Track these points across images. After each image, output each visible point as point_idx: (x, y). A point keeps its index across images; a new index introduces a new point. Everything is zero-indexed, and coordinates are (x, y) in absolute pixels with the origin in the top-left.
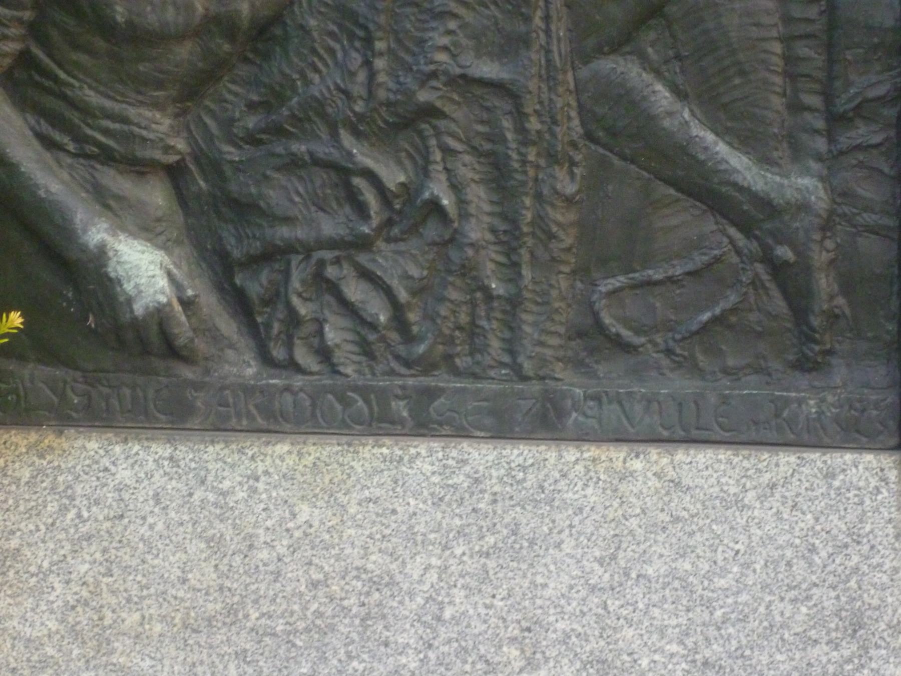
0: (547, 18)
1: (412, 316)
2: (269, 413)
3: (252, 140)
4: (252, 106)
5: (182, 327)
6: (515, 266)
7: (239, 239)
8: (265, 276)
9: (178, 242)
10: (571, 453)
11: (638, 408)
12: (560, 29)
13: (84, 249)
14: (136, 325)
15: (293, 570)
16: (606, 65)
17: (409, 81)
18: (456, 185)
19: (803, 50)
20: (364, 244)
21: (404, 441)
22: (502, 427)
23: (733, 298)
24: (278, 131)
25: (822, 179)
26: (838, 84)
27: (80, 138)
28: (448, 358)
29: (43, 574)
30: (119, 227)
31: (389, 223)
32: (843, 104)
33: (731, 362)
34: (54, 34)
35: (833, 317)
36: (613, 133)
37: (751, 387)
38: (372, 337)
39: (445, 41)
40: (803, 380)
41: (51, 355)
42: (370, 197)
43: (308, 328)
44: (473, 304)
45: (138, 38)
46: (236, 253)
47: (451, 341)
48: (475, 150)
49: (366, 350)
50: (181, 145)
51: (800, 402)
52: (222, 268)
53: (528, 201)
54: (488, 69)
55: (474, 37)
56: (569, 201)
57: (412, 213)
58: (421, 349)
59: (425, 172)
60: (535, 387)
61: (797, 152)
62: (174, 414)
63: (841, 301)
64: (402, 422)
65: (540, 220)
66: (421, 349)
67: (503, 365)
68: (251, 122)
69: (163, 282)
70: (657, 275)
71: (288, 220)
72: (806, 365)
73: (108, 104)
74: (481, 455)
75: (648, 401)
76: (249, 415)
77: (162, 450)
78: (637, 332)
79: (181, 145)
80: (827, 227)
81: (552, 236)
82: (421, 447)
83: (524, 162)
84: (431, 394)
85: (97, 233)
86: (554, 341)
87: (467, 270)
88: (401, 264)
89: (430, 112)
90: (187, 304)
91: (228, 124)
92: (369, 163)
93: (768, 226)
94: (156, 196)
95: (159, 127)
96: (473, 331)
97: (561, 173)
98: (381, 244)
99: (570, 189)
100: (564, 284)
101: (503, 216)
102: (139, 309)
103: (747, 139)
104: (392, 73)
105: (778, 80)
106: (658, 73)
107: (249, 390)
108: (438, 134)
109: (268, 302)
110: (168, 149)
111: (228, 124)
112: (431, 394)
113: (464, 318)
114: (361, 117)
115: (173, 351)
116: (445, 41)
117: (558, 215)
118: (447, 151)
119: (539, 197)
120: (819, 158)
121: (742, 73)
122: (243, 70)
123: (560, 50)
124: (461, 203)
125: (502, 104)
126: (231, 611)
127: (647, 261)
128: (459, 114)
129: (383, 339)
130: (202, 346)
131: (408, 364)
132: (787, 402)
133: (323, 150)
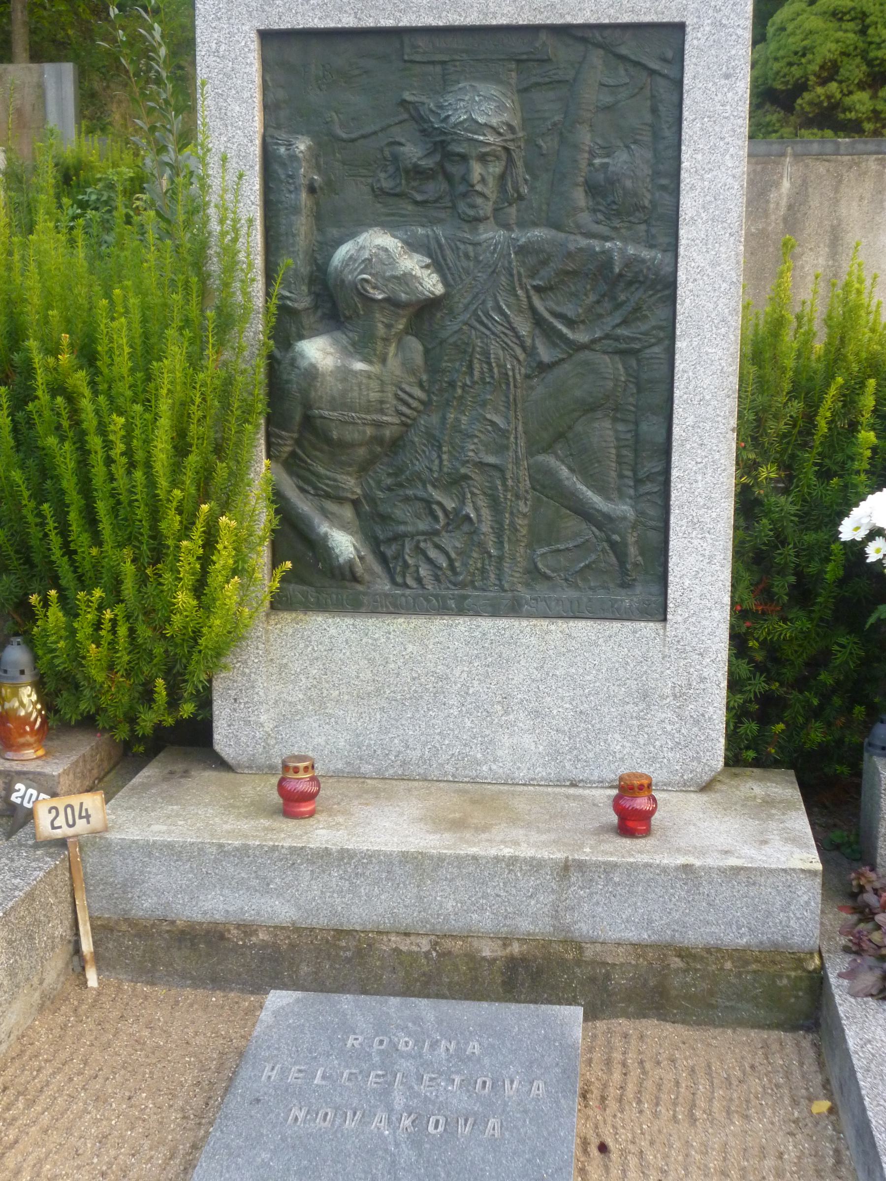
0: (516, 438)
1: (457, 564)
2: (395, 606)
3: (389, 489)
4: (389, 475)
5: (359, 569)
6: (501, 543)
7: (383, 531)
8: (394, 547)
9: (357, 533)
10: (525, 623)
11: (553, 603)
12: (522, 443)
13: (318, 534)
14: (340, 567)
15: (405, 673)
16: (541, 458)
17: (457, 464)
18: (477, 509)
19: (625, 452)
20: (436, 533)
21: (453, 618)
22: (495, 612)
24: (401, 485)
25: (632, 506)
26: (639, 466)
27: (316, 488)
28: (472, 582)
29: (297, 674)
30: (332, 525)
31: (448, 524)
32: (641, 475)
33: (592, 584)
34: (306, 443)
35: (636, 565)
36: (544, 487)
37: (601, 595)
38: (440, 573)
39: (472, 447)
40: (623, 592)
41: (302, 581)
42: (440, 514)
43: (412, 569)
44: (483, 559)
45: (343, 445)
46: (381, 537)
47: (473, 575)
48: (485, 494)
49: (437, 579)
50: (359, 491)
51: (622, 601)
52: (374, 543)
53: (507, 515)
54: (491, 459)
55: (485, 445)
56: (525, 515)
58: (461, 578)
59: (463, 503)
60: (510, 594)
61: (622, 496)
62: (354, 606)
63: (640, 558)
64: (452, 610)
65: (512, 524)
66: (461, 578)
67: (495, 585)
68: (389, 481)
69: (352, 549)
70: (561, 547)
71: (405, 523)
72: (624, 585)
73: (328, 473)
74: (486, 624)
75: (558, 600)
76: (387, 606)
77: (349, 621)
78: (553, 571)
79: (359, 491)
80: (634, 527)
81: (517, 530)
82: (460, 620)
83: (506, 499)
84: (465, 597)
85: (324, 528)
86: (517, 575)
87: (481, 545)
88: (452, 542)
89: (466, 477)
90: (361, 558)
91: (379, 482)
92: (439, 499)
93: (609, 526)
94: (348, 513)
95: (350, 484)
96: (483, 571)
97: (521, 503)
98: (444, 533)
99: (525, 510)
100: (522, 550)
101: (496, 522)
102: (341, 560)
103: (602, 489)
104: (450, 461)
105: (614, 465)
106: (563, 462)
107: (386, 596)
108: (469, 487)
110: (353, 493)
111: (379, 482)
112: (465, 597)
113: (479, 565)
114: (436, 479)
115: (355, 579)
116: (472, 447)
117: (520, 521)
118: (473, 494)
119: (512, 513)
120: (631, 498)
121: (599, 462)
122: (386, 460)
124: (479, 515)
125: (496, 474)
126: (378, 690)
127: (558, 541)
128: (477, 477)
129: (444, 574)
130: (367, 577)
131: (455, 585)
132: (616, 601)
133: (420, 493)
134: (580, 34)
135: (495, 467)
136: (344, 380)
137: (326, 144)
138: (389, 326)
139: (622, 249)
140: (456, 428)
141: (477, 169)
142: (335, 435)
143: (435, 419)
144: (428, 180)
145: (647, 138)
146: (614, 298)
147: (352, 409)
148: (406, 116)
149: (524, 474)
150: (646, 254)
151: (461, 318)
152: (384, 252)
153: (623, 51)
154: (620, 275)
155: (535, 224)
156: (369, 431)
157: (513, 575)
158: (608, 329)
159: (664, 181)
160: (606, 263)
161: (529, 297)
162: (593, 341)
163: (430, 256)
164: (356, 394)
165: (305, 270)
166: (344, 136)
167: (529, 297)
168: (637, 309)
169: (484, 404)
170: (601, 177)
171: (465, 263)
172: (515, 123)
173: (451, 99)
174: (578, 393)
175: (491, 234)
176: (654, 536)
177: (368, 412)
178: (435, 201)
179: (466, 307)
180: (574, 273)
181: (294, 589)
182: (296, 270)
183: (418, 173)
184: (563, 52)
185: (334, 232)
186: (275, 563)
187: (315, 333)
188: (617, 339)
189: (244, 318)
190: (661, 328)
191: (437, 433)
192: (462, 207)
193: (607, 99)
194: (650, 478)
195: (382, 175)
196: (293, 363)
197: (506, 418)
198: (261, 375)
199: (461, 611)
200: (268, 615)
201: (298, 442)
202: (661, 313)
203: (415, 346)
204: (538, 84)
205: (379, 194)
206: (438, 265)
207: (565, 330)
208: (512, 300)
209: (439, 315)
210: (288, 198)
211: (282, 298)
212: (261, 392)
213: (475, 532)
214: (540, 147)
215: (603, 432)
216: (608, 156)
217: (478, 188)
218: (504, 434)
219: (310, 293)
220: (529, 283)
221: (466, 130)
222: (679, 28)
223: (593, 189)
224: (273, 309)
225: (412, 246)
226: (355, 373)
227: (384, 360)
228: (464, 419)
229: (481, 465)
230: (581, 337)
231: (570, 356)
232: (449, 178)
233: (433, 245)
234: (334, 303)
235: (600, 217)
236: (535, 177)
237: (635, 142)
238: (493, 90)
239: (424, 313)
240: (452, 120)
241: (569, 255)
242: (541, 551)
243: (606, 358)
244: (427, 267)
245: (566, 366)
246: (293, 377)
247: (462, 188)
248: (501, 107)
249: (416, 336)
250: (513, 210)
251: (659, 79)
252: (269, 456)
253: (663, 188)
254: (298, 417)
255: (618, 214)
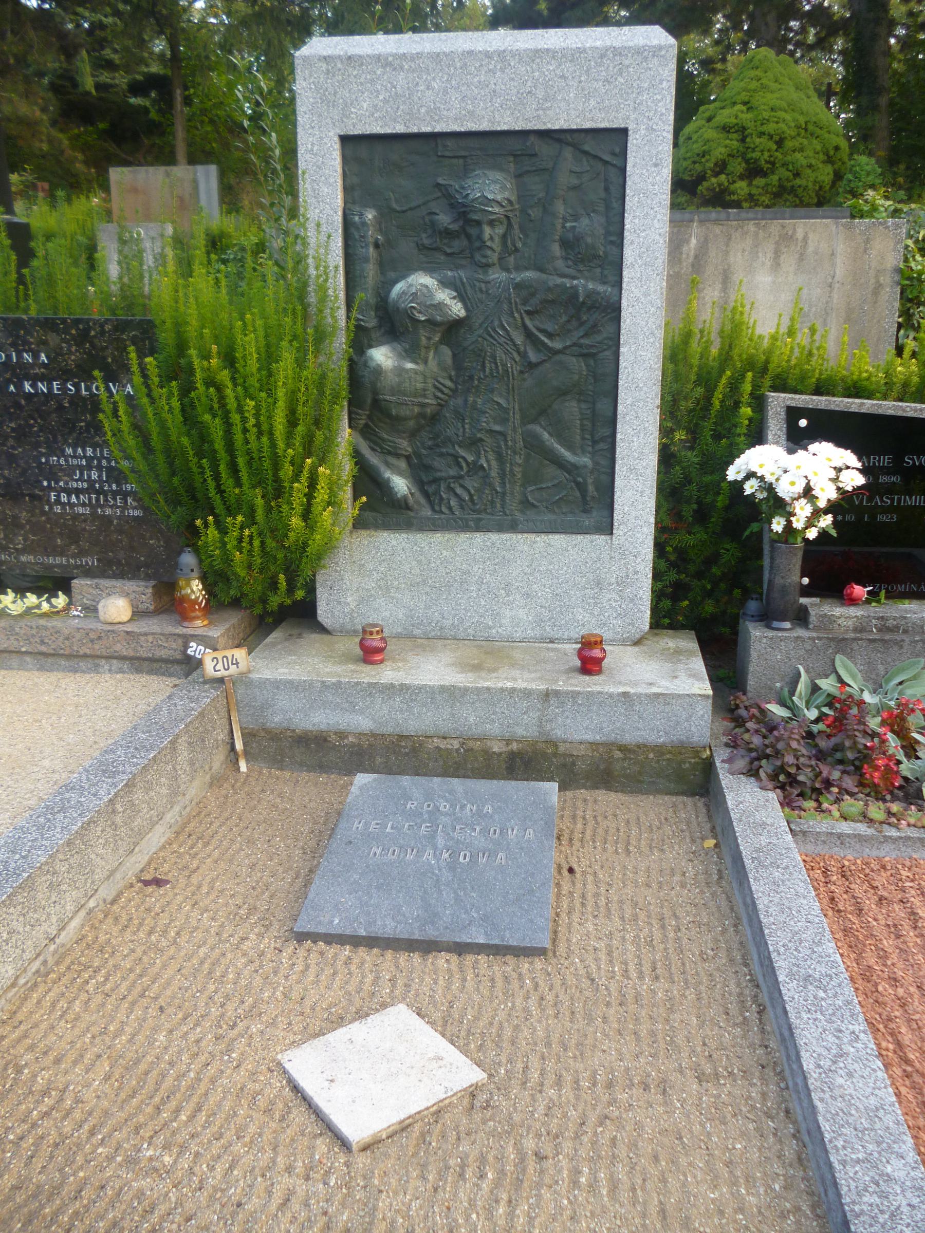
3: (430, 448)
10: (520, 536)
12: (517, 416)
14: (398, 500)
15: (442, 569)
16: (531, 427)
18: (489, 461)
19: (586, 422)
20: (461, 477)
22: (500, 529)
23: (564, 493)
24: (438, 446)
27: (381, 448)
29: (371, 571)
30: (393, 473)
32: (596, 438)
35: (593, 497)
37: (570, 518)
40: (584, 515)
41: (373, 510)
42: (464, 465)
45: (398, 419)
49: (462, 508)
54: (497, 428)
56: (520, 465)
57: (475, 469)
61: (584, 451)
65: (511, 470)
68: (430, 443)
72: (585, 511)
74: (494, 537)
75: (542, 521)
77: (404, 536)
82: (478, 535)
84: (480, 520)
85: (387, 474)
87: (491, 485)
88: (472, 483)
89: (481, 440)
90: (412, 494)
91: (423, 443)
94: (403, 464)
95: (404, 445)
96: (492, 502)
97: (517, 457)
103: (570, 447)
107: (429, 519)
109: (434, 494)
111: (423, 443)
112: (480, 520)
115: (408, 508)
122: (427, 429)
123: (518, 422)
126: (424, 581)
128: (488, 440)
133: (451, 451)
134: (556, 136)
135: (499, 433)
136: (399, 375)
137: (386, 213)
138: (429, 339)
139: (584, 285)
140: (474, 407)
141: (487, 231)
142: (394, 412)
143: (460, 401)
144: (454, 238)
145: (601, 209)
146: (579, 319)
147: (405, 395)
148: (439, 194)
149: (519, 437)
150: (601, 288)
151: (477, 333)
152: (426, 288)
153: (586, 147)
154: (583, 303)
155: (527, 269)
156: (416, 410)
157: (512, 504)
158: (575, 339)
159: (613, 238)
160: (573, 294)
161: (522, 318)
162: (566, 348)
163: (456, 291)
164: (407, 385)
165: (373, 301)
166: (398, 209)
167: (522, 318)
168: (595, 326)
169: (492, 391)
170: (570, 236)
171: (479, 295)
172: (513, 198)
173: (469, 182)
174: (555, 383)
175: (497, 276)
176: (604, 478)
177: (415, 397)
178: (460, 253)
179: (481, 325)
180: (553, 302)
181: (368, 514)
182: (367, 301)
183: (448, 234)
184: (545, 149)
185: (392, 275)
186: (356, 498)
187: (380, 344)
188: (581, 346)
189: (333, 334)
190: (610, 339)
191: (461, 411)
192: (478, 257)
193: (575, 181)
194: (603, 439)
195: (424, 235)
196: (366, 364)
197: (507, 400)
198: (344, 372)
199: (478, 529)
200: (351, 532)
201: (370, 417)
202: (611, 328)
203: (446, 351)
204: (528, 172)
205: (422, 248)
206: (461, 297)
207: (546, 340)
208: (511, 320)
209: (462, 331)
210: (360, 251)
211: (358, 320)
212: (344, 384)
213: (487, 476)
214: (529, 215)
215: (572, 409)
216: (575, 221)
217: (488, 244)
218: (506, 410)
219: (376, 316)
220: (522, 309)
221: (480, 204)
222: (625, 131)
223: (565, 244)
224: (352, 328)
225: (444, 283)
226: (407, 371)
227: (426, 362)
228: (479, 401)
229: (491, 432)
230: (557, 345)
231: (550, 358)
232: (468, 237)
233: (458, 283)
234: (392, 323)
235: (570, 263)
236: (526, 236)
237: (594, 211)
238: (498, 176)
239: (452, 330)
240: (471, 197)
241: (549, 289)
242: (530, 489)
243: (574, 359)
244: (454, 298)
245: (547, 365)
246: (366, 373)
247: (477, 244)
248: (503, 188)
249: (447, 345)
250: (511, 259)
251: (610, 168)
252: (350, 427)
253: (612, 242)
254: (369, 401)
255: (582, 261)
